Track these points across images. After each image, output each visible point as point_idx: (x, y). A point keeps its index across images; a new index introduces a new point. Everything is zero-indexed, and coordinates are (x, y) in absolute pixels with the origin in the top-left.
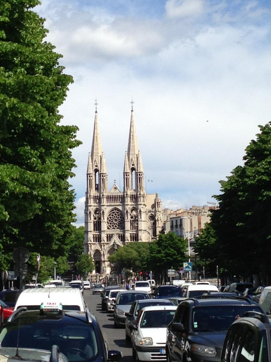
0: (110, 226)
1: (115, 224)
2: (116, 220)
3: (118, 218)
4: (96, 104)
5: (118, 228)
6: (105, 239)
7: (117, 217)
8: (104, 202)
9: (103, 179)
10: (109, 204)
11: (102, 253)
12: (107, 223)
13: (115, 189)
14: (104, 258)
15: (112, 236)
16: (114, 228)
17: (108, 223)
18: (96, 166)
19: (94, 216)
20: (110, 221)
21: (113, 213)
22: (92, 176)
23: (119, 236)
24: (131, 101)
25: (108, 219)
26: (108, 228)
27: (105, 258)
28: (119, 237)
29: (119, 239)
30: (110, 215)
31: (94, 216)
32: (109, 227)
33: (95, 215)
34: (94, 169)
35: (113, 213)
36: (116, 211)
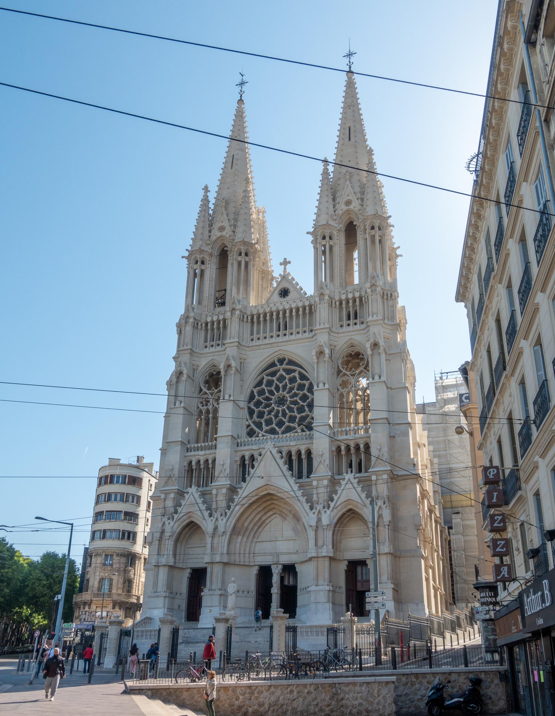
0: (259, 425)
3: (292, 389)
4: (242, 84)
5: (289, 429)
9: (239, 263)
16: (273, 432)
17: (251, 412)
20: (258, 404)
21: (273, 374)
26: (251, 433)
29: (291, 469)
30: (260, 383)
31: (201, 390)
32: (253, 426)
33: (205, 390)
35: (273, 374)
36: (284, 366)
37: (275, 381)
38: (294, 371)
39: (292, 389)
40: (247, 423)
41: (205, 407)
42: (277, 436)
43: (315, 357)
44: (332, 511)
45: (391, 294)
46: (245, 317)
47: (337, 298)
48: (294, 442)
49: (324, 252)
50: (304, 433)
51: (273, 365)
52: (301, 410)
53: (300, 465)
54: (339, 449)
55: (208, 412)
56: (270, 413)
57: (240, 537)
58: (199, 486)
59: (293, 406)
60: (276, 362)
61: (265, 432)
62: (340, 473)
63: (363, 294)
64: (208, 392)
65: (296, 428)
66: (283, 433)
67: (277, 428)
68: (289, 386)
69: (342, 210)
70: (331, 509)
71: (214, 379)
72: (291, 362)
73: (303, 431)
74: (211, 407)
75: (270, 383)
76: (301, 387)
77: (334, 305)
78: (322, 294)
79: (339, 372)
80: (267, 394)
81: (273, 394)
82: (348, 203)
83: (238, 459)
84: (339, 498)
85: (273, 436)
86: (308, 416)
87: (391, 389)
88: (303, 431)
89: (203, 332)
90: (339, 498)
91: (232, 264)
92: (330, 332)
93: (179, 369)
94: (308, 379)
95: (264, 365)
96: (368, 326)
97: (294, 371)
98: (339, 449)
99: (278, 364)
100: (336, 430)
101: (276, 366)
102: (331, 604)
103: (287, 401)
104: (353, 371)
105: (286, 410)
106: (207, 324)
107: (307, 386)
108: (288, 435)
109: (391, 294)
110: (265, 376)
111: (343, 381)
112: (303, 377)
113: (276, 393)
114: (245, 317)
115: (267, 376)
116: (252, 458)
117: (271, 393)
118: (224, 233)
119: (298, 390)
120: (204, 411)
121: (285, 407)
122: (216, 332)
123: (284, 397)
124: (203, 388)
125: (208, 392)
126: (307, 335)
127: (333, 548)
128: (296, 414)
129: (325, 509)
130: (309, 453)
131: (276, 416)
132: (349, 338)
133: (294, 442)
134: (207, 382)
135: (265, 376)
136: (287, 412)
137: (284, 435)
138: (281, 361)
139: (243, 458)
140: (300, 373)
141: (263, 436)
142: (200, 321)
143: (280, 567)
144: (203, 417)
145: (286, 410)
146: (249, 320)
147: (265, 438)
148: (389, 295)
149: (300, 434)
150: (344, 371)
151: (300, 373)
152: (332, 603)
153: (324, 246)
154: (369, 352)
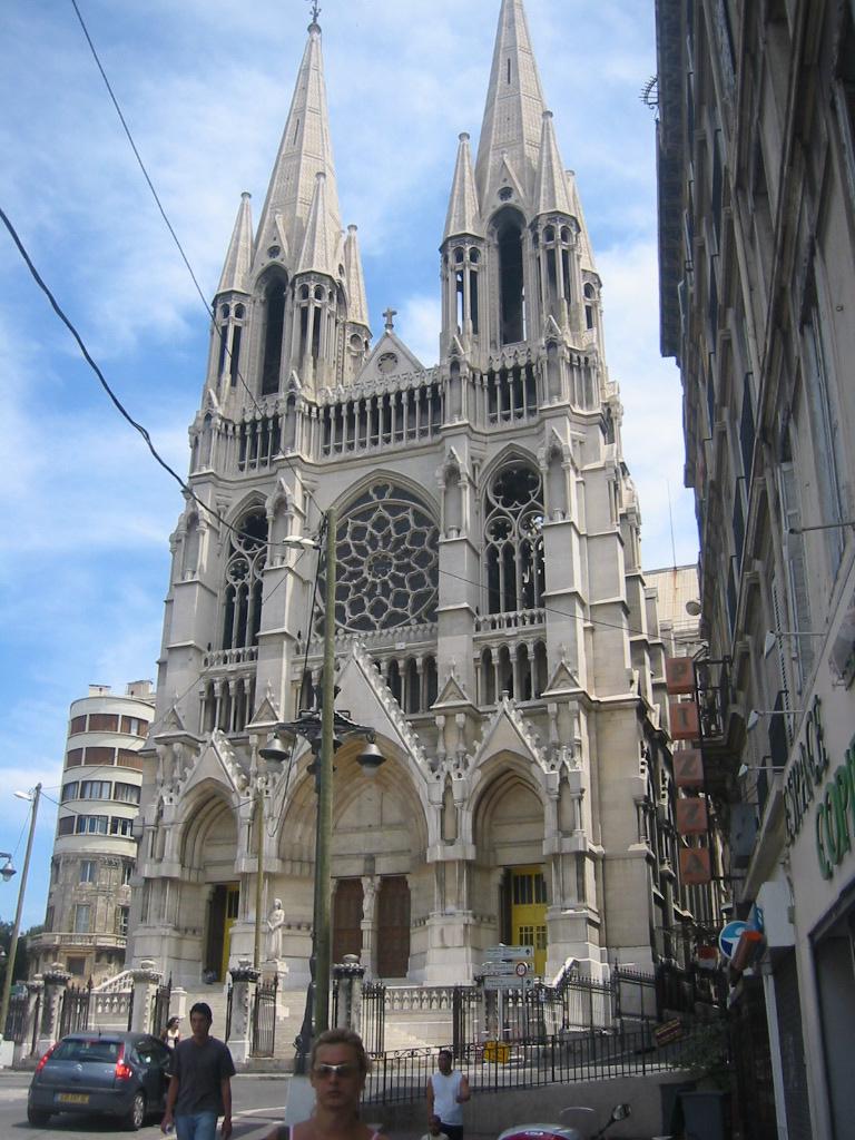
1: (370, 595)
2: (380, 565)
3: (400, 542)
5: (395, 619)
8: (302, 443)
9: (304, 311)
11: (245, 812)
13: (389, 362)
14: (257, 852)
16: (364, 624)
17: (322, 586)
19: (232, 550)
21: (365, 515)
27: (269, 845)
28: (393, 683)
29: (396, 693)
31: (232, 550)
33: (240, 549)
35: (365, 515)
37: (370, 529)
38: (406, 508)
39: (400, 542)
40: (316, 609)
41: (240, 582)
42: (370, 633)
43: (441, 482)
44: (473, 772)
45: (586, 359)
46: (314, 409)
47: (485, 370)
48: (402, 641)
49: (460, 287)
50: (421, 626)
51: (365, 497)
52: (417, 581)
53: (412, 682)
54: (487, 654)
55: (244, 590)
57: (300, 826)
58: (225, 729)
59: (401, 574)
60: (371, 493)
61: (350, 626)
62: (489, 700)
63: (534, 361)
64: (244, 552)
65: (407, 617)
66: (384, 626)
67: (372, 618)
68: (395, 535)
69: (494, 207)
70: (469, 769)
71: (255, 527)
72: (399, 492)
73: (420, 621)
74: (250, 580)
75: (359, 533)
76: (417, 538)
77: (478, 382)
78: (455, 366)
79: (489, 507)
80: (354, 554)
81: (365, 553)
82: (506, 193)
83: (298, 677)
84: (485, 747)
85: (363, 633)
86: (430, 592)
87: (588, 538)
88: (420, 621)
89: (238, 442)
90: (485, 747)
91: (292, 314)
92: (470, 433)
93: (191, 510)
94: (430, 523)
95: (347, 500)
96: (543, 420)
97: (406, 508)
98: (487, 654)
99: (375, 496)
100: (481, 619)
101: (371, 499)
102: (470, 949)
103: (390, 564)
104: (516, 506)
105: (390, 582)
106: (243, 425)
107: (428, 535)
108: (392, 630)
109: (586, 359)
110: (350, 520)
111: (495, 524)
112: (421, 519)
113: (370, 551)
114: (314, 409)
115: (354, 518)
117: (362, 550)
118: (277, 259)
119: (411, 543)
120: (237, 589)
121: (386, 578)
122: (261, 439)
123: (385, 557)
124: (236, 545)
125: (244, 552)
126: (428, 440)
127: (475, 842)
128: (408, 589)
129: (459, 770)
130: (430, 662)
132: (508, 443)
133: (402, 641)
135: (350, 520)
136: (391, 585)
137: (385, 631)
138: (380, 491)
140: (416, 512)
141: (346, 632)
142: (230, 421)
143: (377, 880)
144: (235, 599)
145: (390, 582)
146: (322, 417)
147: (348, 636)
148: (583, 360)
149: (414, 628)
150: (499, 506)
151: (416, 512)
152: (472, 947)
153: (461, 273)
154: (543, 467)
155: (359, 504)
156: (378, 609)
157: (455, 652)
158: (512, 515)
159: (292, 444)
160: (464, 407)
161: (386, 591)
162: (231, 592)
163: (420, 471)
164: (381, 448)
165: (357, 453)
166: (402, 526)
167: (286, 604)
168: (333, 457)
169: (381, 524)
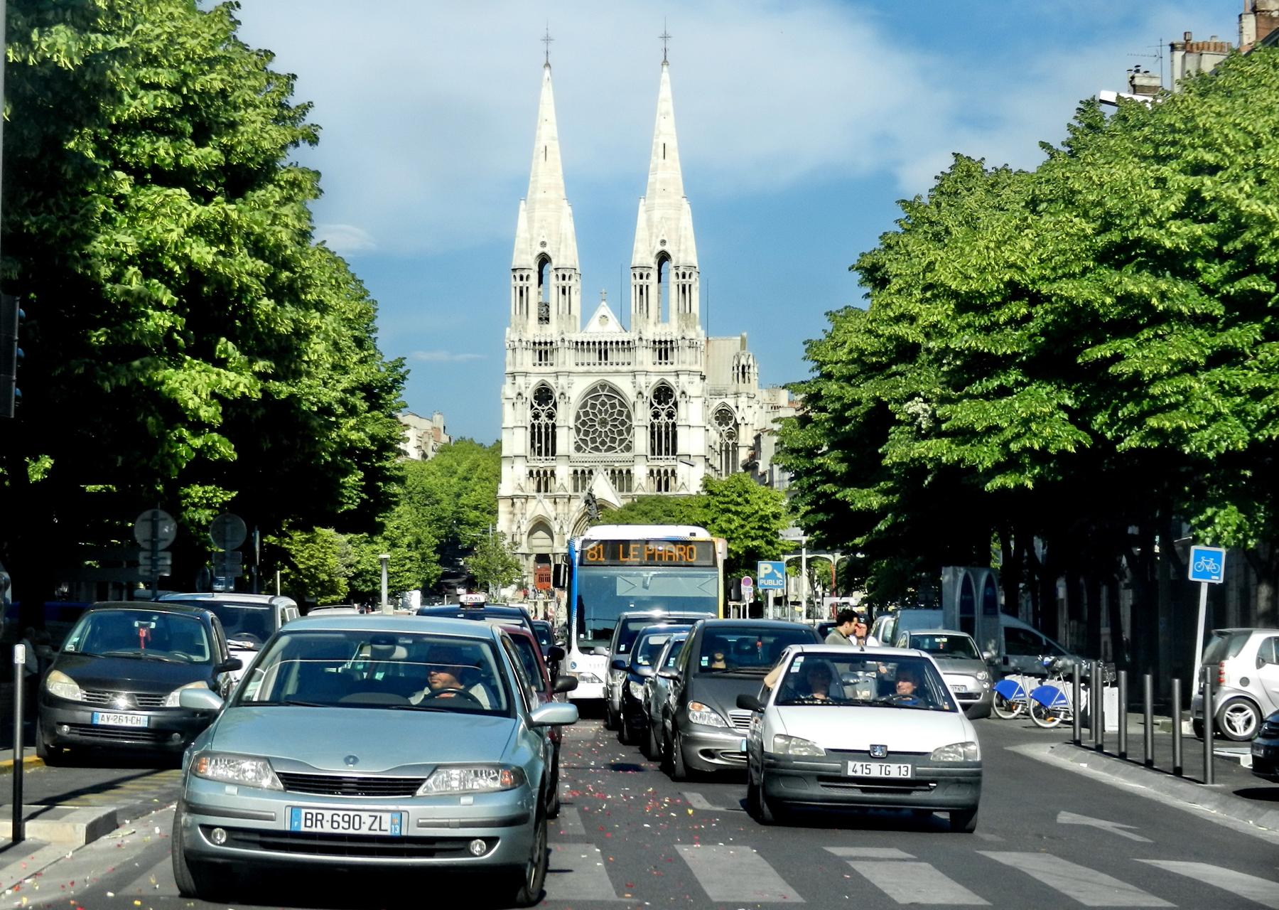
0: (584, 441)
2: (603, 423)
5: (610, 449)
6: (569, 484)
7: (606, 411)
8: (566, 359)
10: (581, 369)
12: (574, 431)
15: (591, 472)
16: (597, 449)
17: (578, 431)
18: (543, 244)
19: (532, 406)
20: (584, 423)
22: (528, 277)
23: (613, 472)
24: (662, 33)
25: (578, 417)
26: (578, 449)
30: (584, 405)
34: (536, 253)
51: (594, 390)
56: (594, 433)
72: (612, 390)
82: (663, 242)
112: (622, 405)
116: (583, 472)
131: (600, 436)
134: (535, 398)
138: (603, 387)
139: (575, 472)
155: (593, 393)
156: (603, 443)
157: (640, 472)
158: (663, 409)
159: (564, 363)
160: (646, 358)
161: (607, 436)
162: (533, 426)
163: (624, 384)
164: (603, 368)
165: (592, 368)
166: (613, 406)
167: (565, 440)
168: (581, 369)
169: (603, 404)
